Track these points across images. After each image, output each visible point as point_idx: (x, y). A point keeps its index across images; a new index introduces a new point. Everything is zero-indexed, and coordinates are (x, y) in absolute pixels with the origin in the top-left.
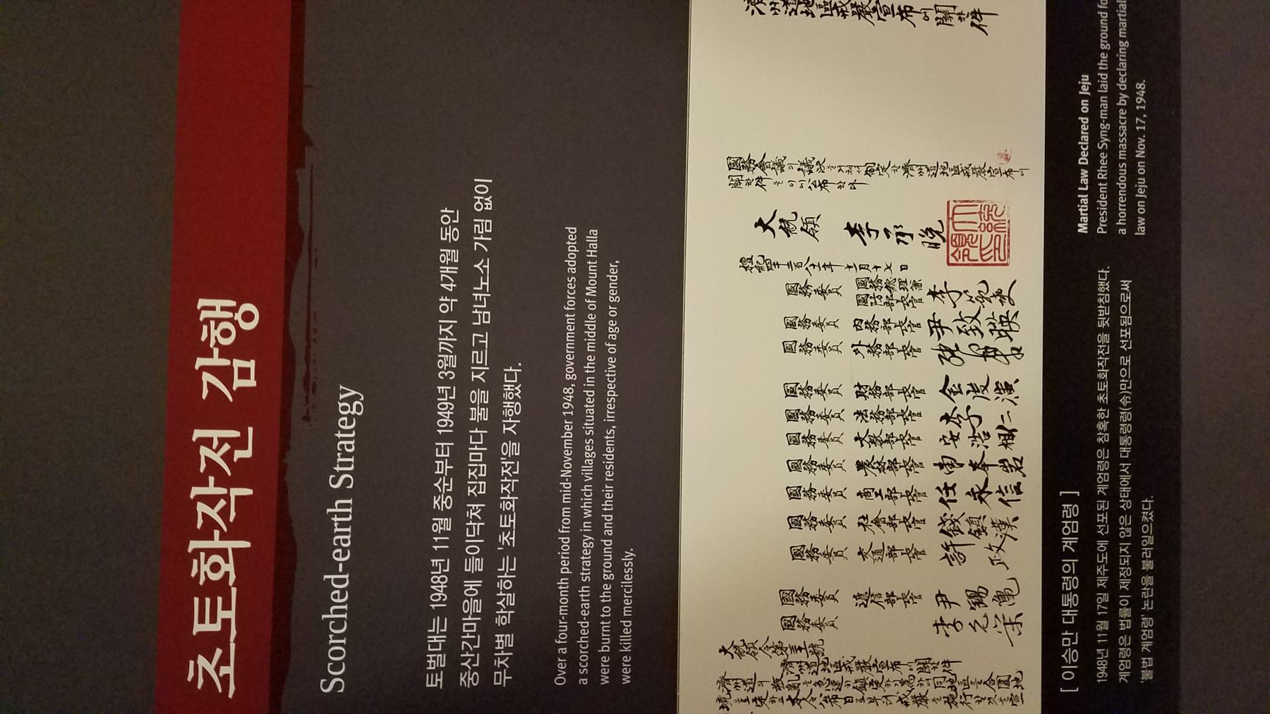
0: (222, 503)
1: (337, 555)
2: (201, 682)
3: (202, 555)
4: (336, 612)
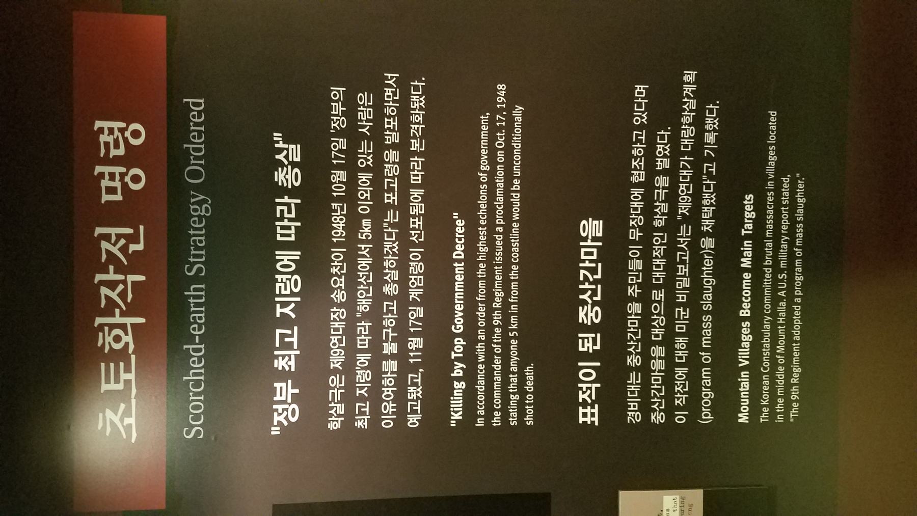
0: (121, 287)
1: (194, 329)
2: (109, 430)
3: (106, 328)
4: (195, 374)
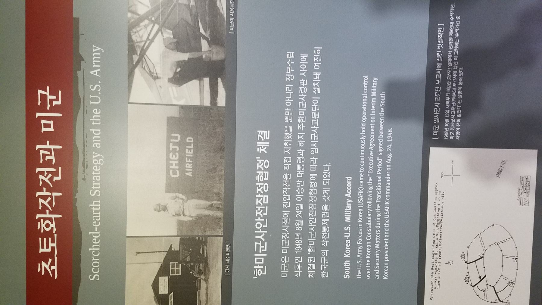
0: (49, 199)
1: (95, 224)
3: (42, 220)
4: (95, 247)
